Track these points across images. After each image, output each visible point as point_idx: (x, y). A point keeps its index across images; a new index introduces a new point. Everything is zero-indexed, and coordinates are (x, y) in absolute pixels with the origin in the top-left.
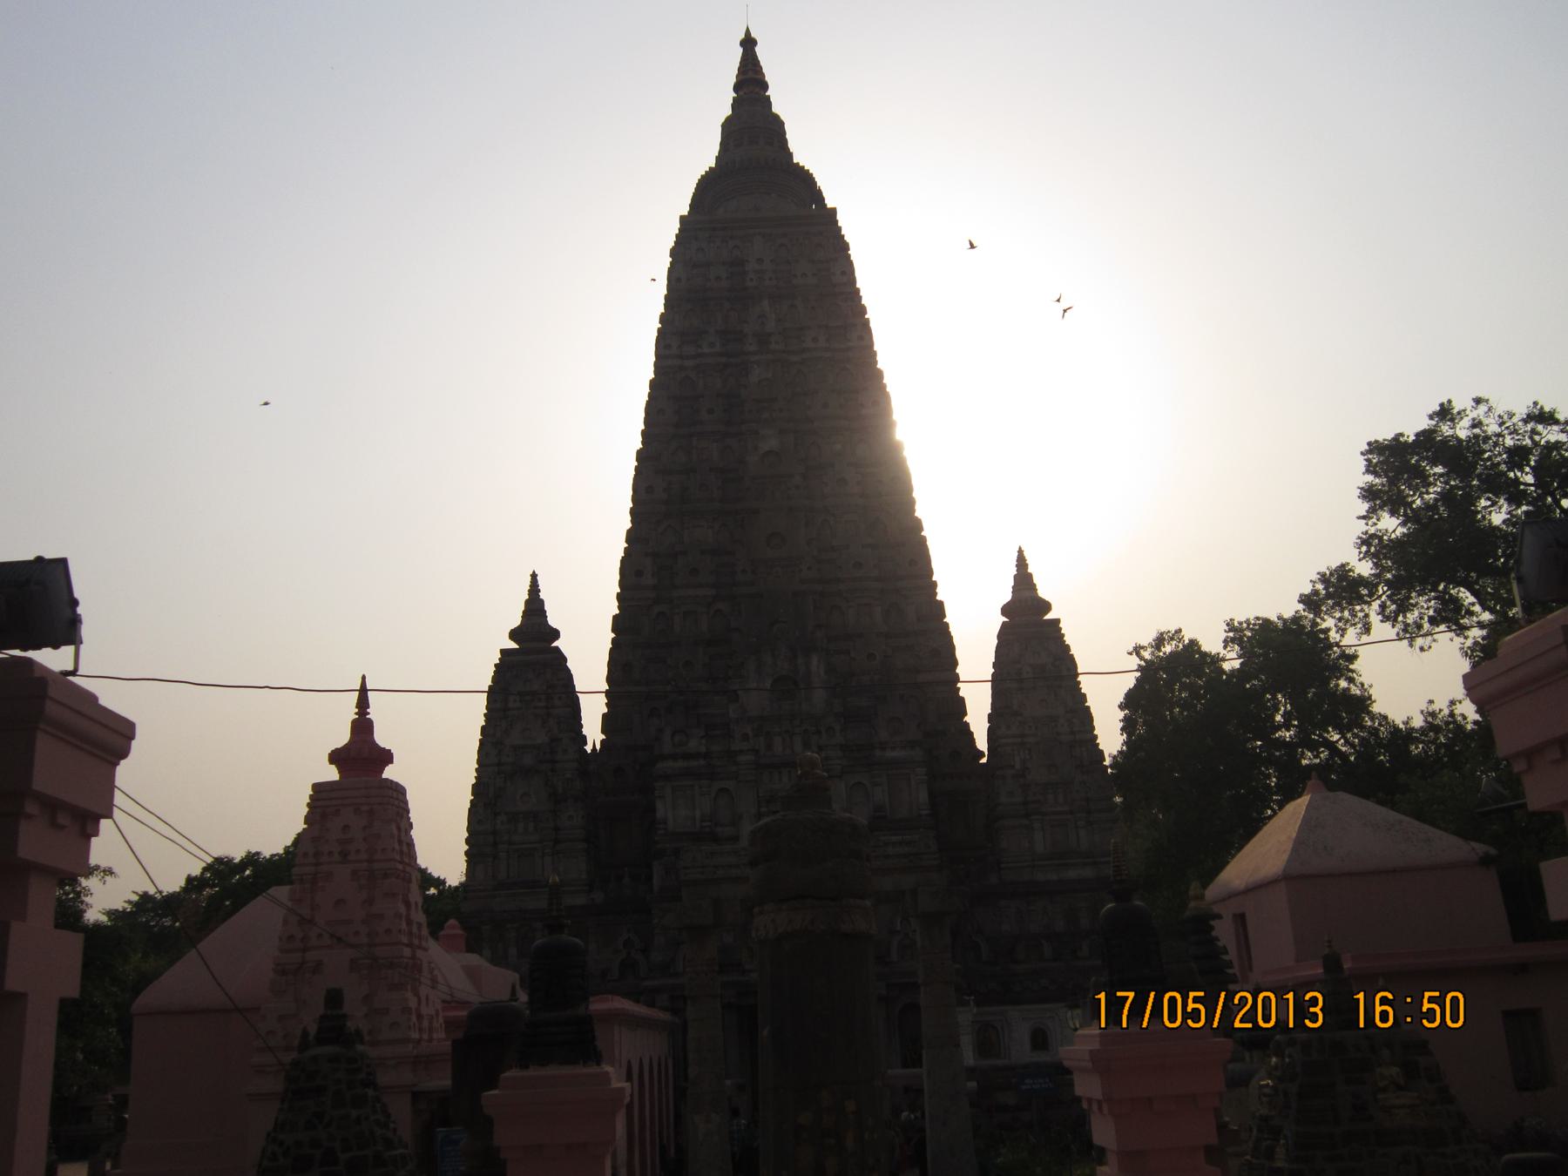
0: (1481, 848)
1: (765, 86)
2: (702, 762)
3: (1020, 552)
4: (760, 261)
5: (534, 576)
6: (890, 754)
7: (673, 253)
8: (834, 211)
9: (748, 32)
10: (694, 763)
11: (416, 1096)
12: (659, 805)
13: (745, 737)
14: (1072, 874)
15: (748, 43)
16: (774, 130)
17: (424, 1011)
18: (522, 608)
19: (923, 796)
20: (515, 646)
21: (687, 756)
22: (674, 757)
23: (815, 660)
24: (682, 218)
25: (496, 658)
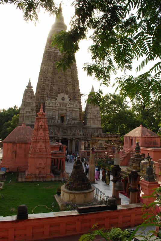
2: (52, 107)
5: (30, 79)
10: (50, 107)
20: (27, 88)
21: (50, 106)
22: (48, 106)
25: (25, 90)
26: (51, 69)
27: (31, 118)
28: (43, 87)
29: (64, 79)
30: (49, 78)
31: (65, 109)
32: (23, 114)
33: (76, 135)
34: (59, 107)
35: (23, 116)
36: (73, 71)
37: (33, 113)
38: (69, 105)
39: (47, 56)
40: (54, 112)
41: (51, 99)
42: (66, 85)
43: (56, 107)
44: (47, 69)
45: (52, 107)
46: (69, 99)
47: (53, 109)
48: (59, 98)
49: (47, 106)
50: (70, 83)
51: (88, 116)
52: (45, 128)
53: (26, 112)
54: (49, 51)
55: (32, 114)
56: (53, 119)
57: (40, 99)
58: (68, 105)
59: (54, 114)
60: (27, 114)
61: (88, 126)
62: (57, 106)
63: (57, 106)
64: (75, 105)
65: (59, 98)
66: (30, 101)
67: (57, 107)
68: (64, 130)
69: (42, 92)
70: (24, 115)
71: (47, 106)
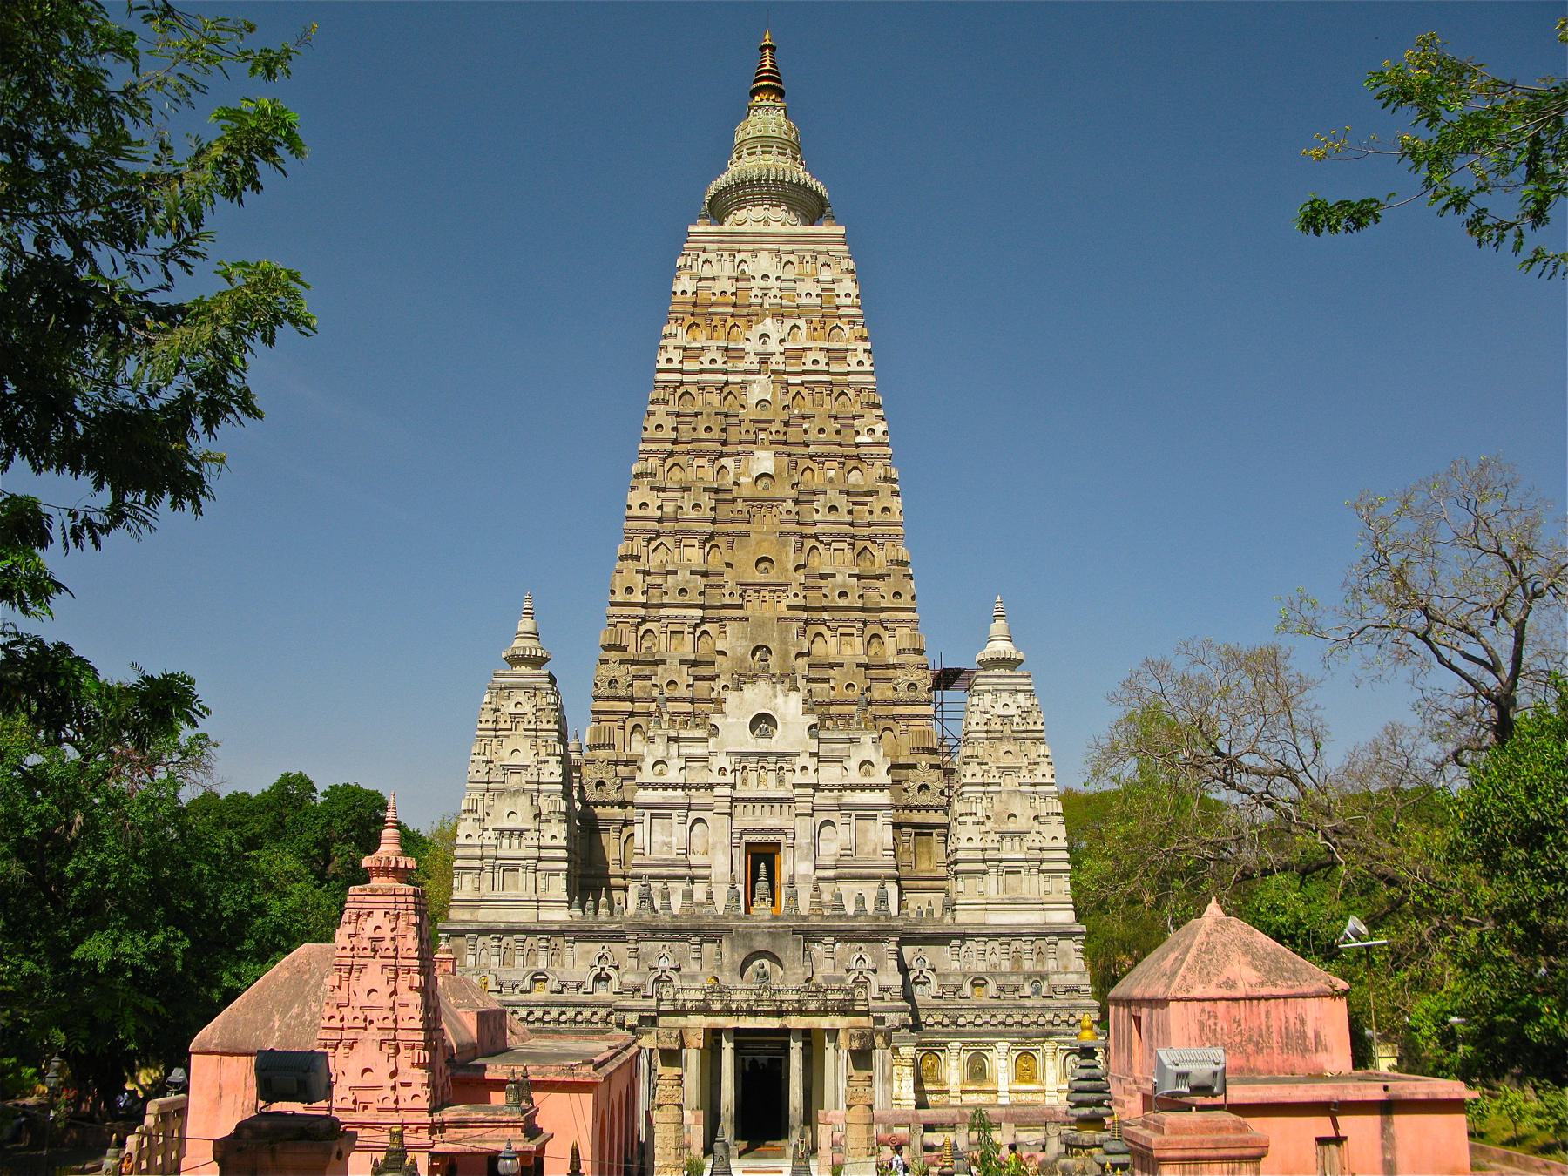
11: (434, 1156)
19: (888, 833)
21: (665, 787)
26: (696, 506)
27: (531, 876)
28: (646, 644)
29: (797, 568)
30: (683, 576)
31: (781, 800)
32: (478, 852)
34: (733, 786)
35: (477, 864)
36: (865, 504)
37: (546, 841)
39: (669, 423)
40: (698, 827)
41: (673, 733)
42: (815, 616)
44: (669, 508)
45: (684, 787)
46: (813, 719)
47: (689, 808)
48: (729, 720)
49: (644, 786)
50: (843, 594)
54: (686, 378)
55: (540, 848)
56: (692, 880)
57: (619, 735)
59: (697, 844)
60: (500, 853)
61: (961, 917)
63: (722, 780)
64: (853, 764)
65: (734, 730)
66: (525, 757)
67: (717, 791)
68: (757, 963)
69: (635, 678)
70: (481, 858)
71: (644, 786)
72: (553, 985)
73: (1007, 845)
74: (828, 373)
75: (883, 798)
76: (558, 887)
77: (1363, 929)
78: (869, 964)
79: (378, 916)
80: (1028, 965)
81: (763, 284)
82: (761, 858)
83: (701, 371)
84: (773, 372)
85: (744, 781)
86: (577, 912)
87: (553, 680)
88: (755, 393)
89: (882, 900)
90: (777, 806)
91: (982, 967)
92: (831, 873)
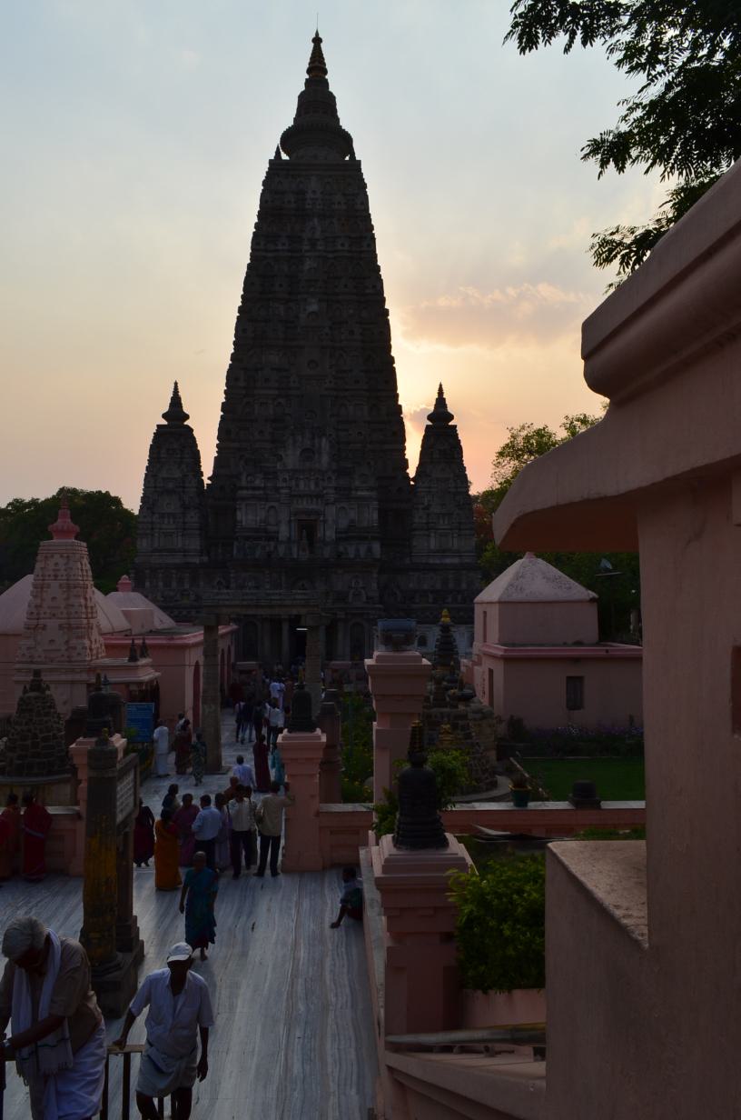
0: (592, 594)
1: (325, 72)
2: (261, 492)
3: (441, 385)
4: (314, 192)
5: (176, 384)
6: (359, 493)
7: (264, 183)
8: (360, 161)
9: (317, 34)
10: (257, 492)
12: (238, 513)
13: (285, 480)
14: (448, 561)
15: (317, 41)
16: (328, 103)
17: (93, 646)
18: (170, 401)
19: (375, 516)
20: (165, 423)
21: (254, 488)
22: (247, 488)
23: (324, 440)
24: (270, 161)
25: (154, 429)
33: (350, 600)
38: (334, 478)
43: (277, 489)
45: (264, 488)
50: (357, 382)
51: (416, 520)
52: (68, 580)
53: (162, 516)
54: (270, 255)
55: (184, 523)
56: (269, 539)
58: (329, 478)
62: (284, 485)
63: (284, 485)
65: (291, 458)
71: (242, 488)
72: (193, 597)
73: (441, 521)
74: (349, 251)
75: (374, 494)
76: (195, 544)
77: (610, 566)
78: (361, 585)
79: (57, 556)
80: (451, 586)
81: (312, 196)
82: (308, 528)
83: (277, 251)
84: (320, 251)
85: (297, 485)
86: (205, 559)
87: (191, 430)
88: (308, 264)
89: (370, 550)
90: (315, 500)
91: (426, 587)
92: (344, 535)
